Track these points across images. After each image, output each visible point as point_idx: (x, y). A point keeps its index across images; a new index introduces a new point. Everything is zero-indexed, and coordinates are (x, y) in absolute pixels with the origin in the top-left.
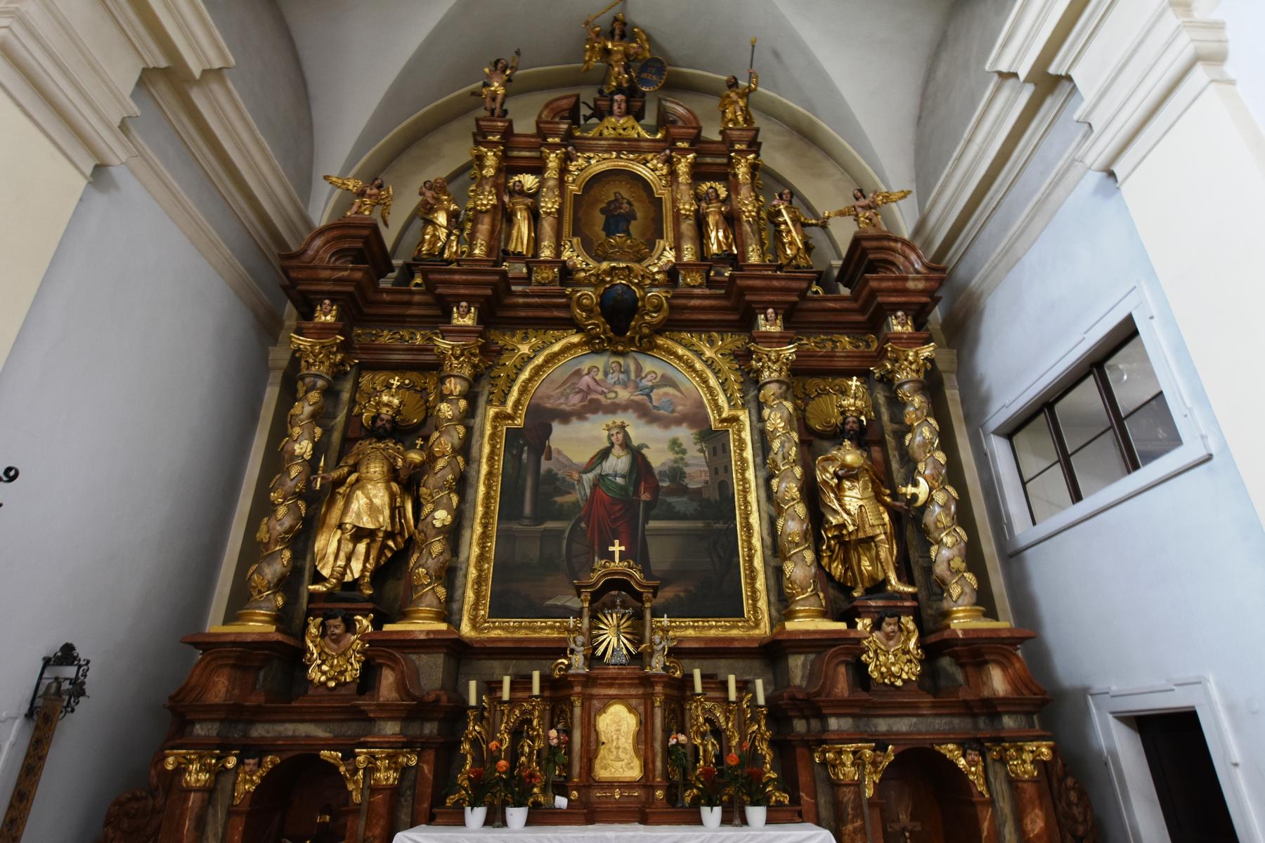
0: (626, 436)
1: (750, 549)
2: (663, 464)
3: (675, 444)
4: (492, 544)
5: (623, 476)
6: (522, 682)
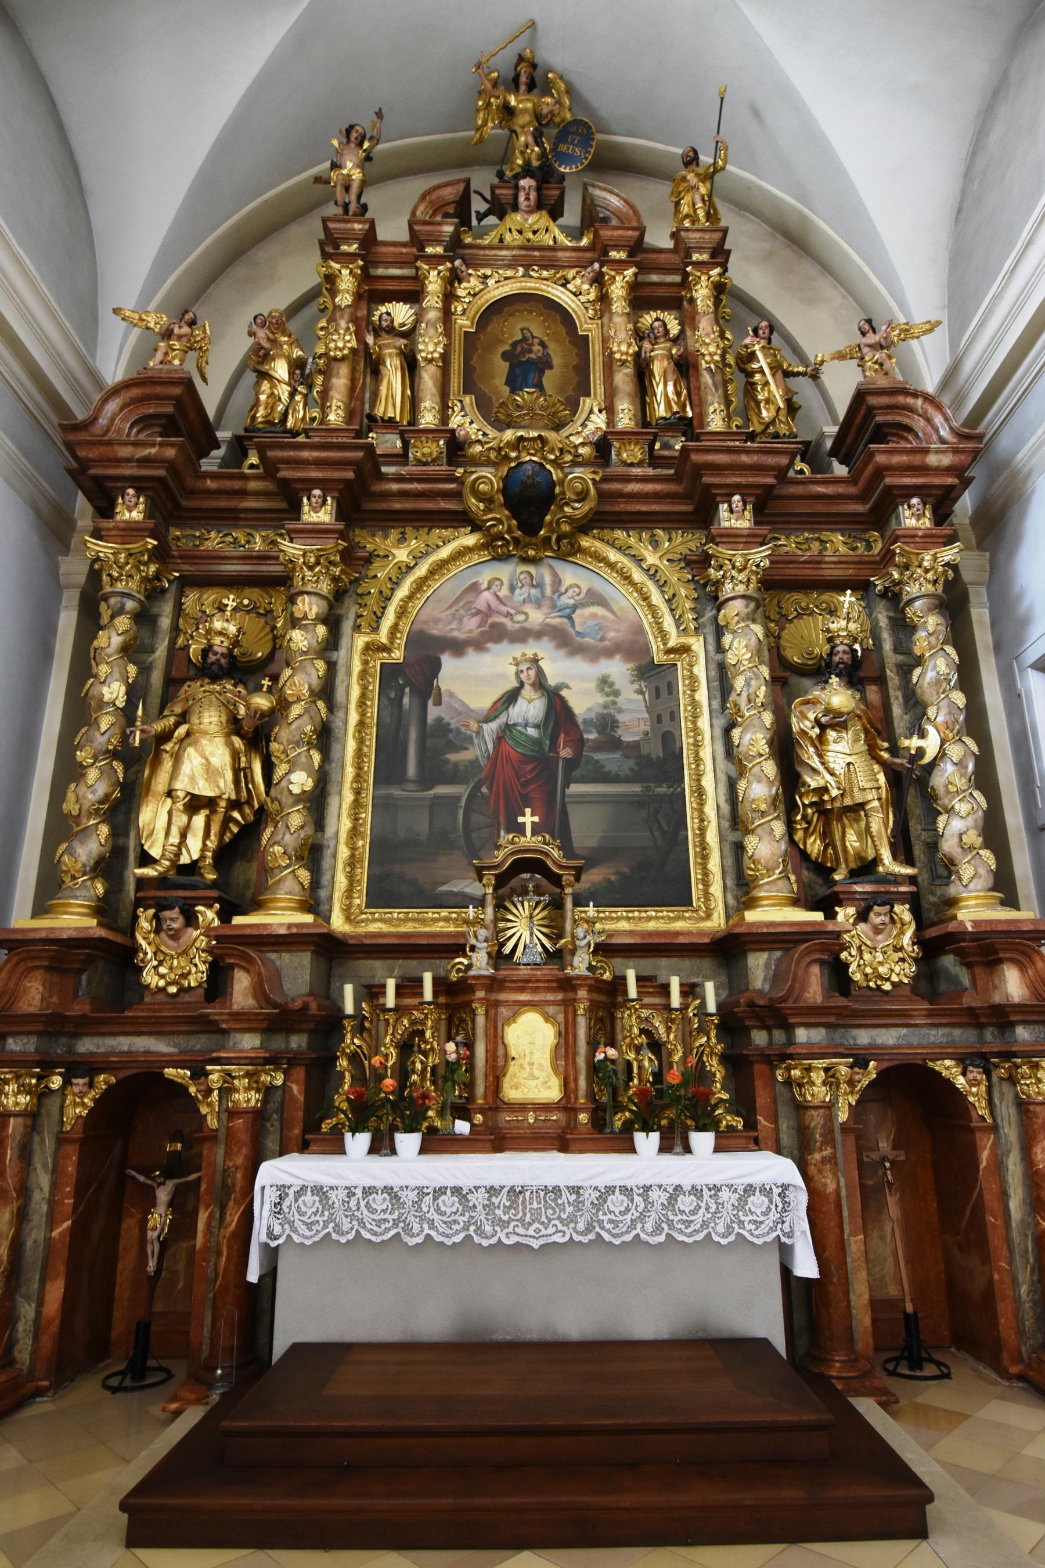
0: (540, 672)
1: (702, 820)
2: (589, 710)
3: (605, 683)
4: (367, 815)
5: (537, 726)
6: (409, 986)
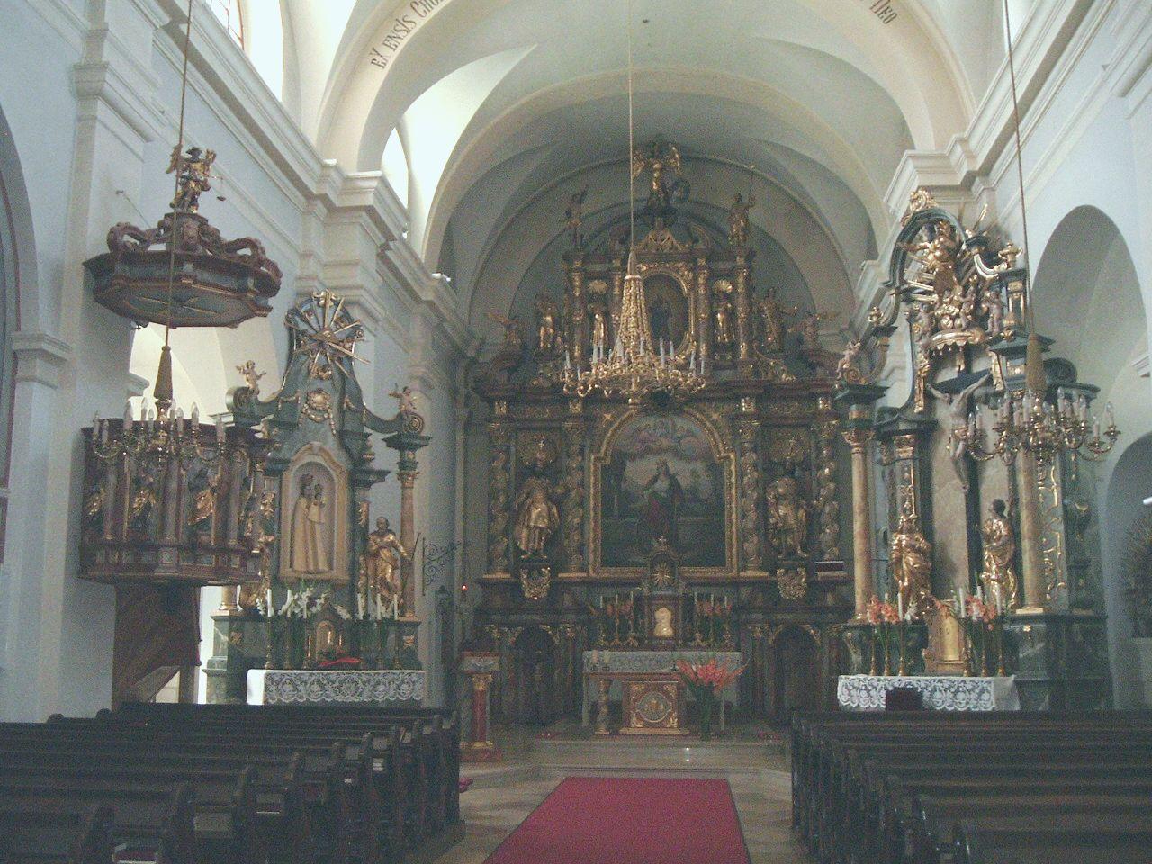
0: (667, 470)
3: (693, 472)
